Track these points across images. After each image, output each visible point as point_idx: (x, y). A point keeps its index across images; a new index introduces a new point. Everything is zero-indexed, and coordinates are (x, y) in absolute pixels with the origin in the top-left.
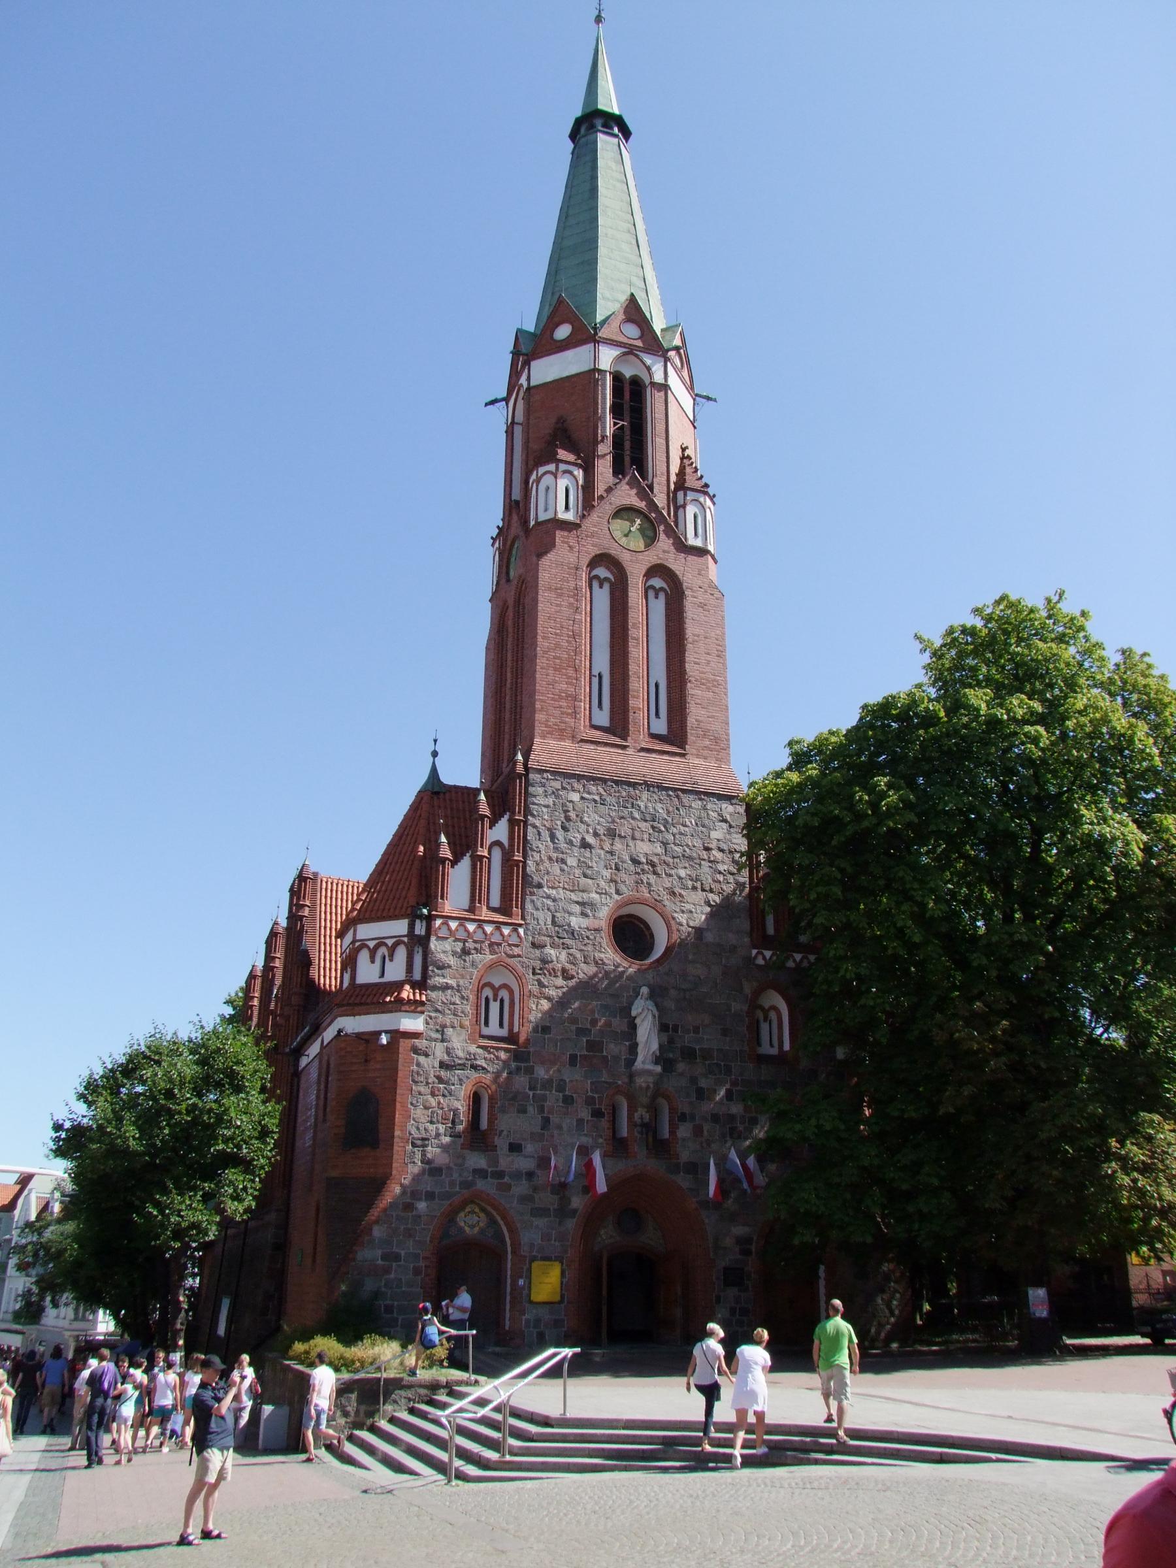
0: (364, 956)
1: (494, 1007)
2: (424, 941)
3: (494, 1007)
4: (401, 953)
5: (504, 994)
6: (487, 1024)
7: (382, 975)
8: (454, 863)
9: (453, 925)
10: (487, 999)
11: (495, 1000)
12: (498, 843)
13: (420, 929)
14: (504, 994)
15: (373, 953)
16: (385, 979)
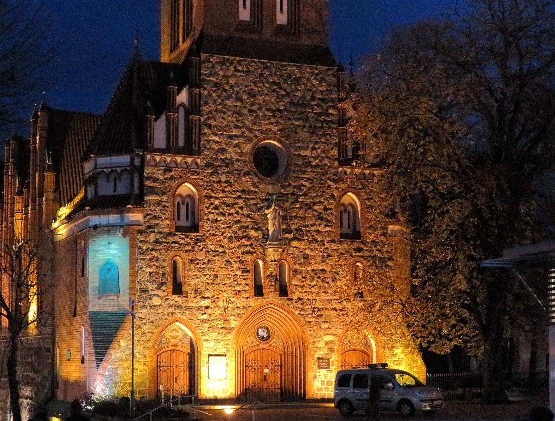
0: (102, 182)
1: (183, 208)
2: (141, 170)
3: (183, 208)
4: (125, 178)
5: (188, 200)
6: (179, 219)
7: (115, 190)
8: (156, 120)
9: (158, 158)
10: (178, 204)
11: (183, 204)
12: (182, 104)
13: (137, 162)
14: (188, 200)
15: (108, 176)
16: (116, 194)
